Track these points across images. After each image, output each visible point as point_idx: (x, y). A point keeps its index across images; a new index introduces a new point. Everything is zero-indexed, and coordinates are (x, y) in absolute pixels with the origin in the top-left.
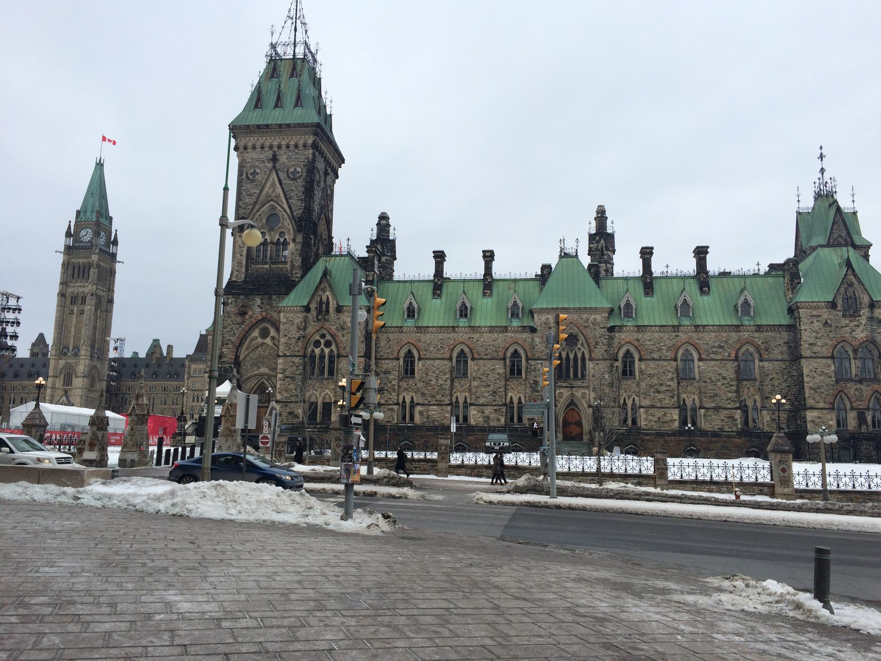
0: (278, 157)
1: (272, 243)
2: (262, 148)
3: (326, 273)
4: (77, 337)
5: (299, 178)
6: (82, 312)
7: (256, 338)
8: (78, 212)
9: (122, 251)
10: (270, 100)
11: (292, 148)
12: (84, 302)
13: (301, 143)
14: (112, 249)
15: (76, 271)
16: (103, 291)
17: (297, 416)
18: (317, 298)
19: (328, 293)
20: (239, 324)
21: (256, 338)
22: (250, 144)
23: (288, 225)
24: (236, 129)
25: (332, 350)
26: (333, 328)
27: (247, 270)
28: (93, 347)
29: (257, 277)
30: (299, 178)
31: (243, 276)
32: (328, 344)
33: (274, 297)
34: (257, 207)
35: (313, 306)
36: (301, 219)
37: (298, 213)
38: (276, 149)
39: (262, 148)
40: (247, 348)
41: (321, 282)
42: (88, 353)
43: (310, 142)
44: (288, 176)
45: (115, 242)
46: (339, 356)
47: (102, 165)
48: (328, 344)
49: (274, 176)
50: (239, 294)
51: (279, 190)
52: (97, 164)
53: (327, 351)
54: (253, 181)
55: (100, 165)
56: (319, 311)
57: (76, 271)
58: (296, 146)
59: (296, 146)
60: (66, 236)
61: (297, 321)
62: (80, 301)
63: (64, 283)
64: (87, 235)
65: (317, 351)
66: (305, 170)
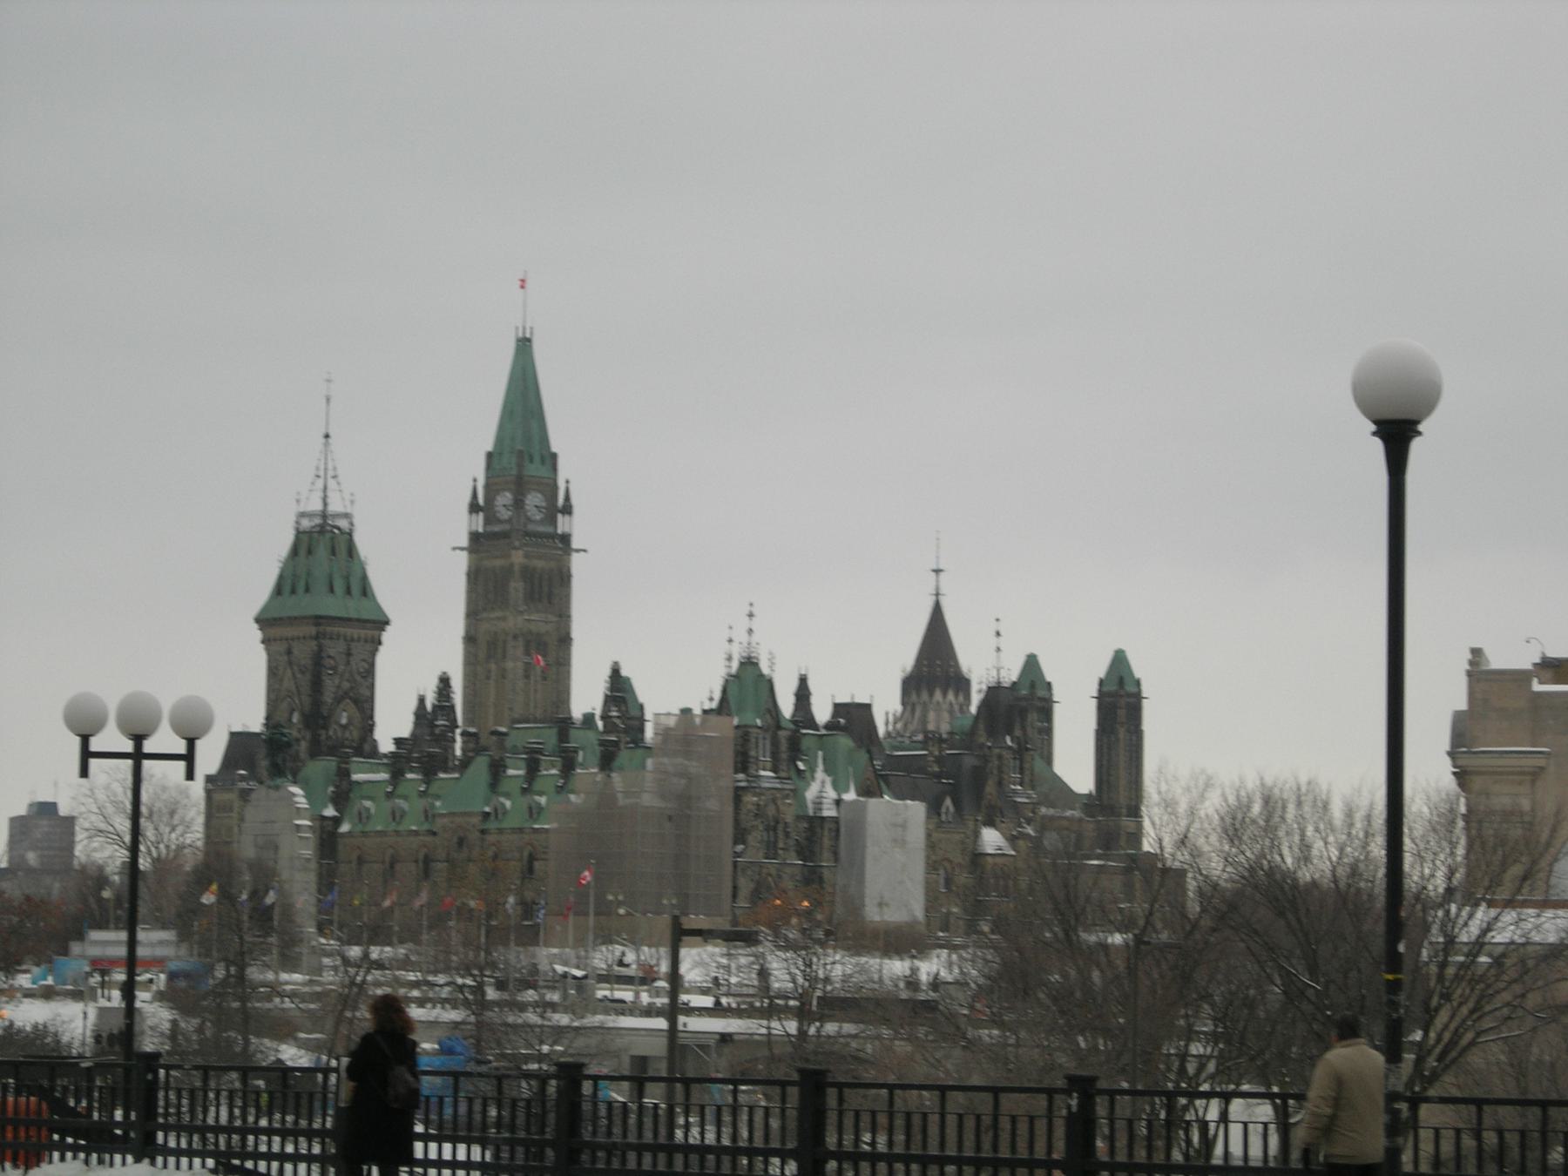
8: (490, 456)
10: (287, 589)
24: (263, 621)
45: (567, 510)
47: (529, 340)
52: (519, 340)
55: (524, 346)
63: (472, 614)
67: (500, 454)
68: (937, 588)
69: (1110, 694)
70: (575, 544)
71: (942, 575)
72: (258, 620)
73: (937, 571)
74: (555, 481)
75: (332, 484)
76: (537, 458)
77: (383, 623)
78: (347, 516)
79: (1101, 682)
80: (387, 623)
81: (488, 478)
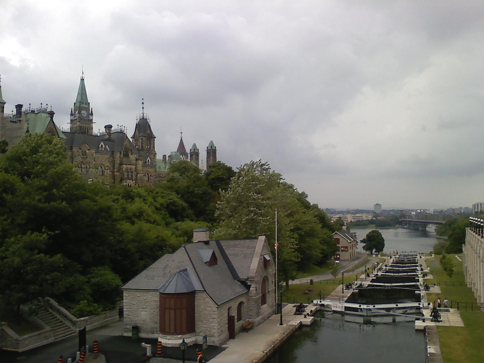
45: (92, 114)
47: (83, 79)
52: (81, 79)
55: (82, 80)
67: (77, 103)
68: (181, 136)
69: (209, 150)
71: (182, 134)
73: (181, 133)
74: (89, 108)
76: (85, 103)
79: (207, 148)
81: (74, 108)
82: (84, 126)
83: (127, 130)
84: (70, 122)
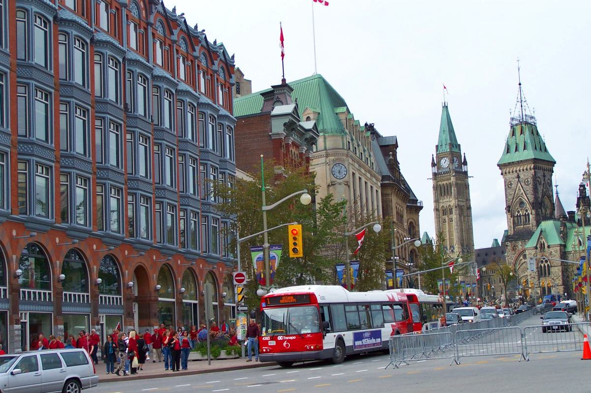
0: (520, 176)
1: (523, 215)
2: (513, 172)
3: (541, 231)
4: (451, 240)
5: (530, 184)
6: (451, 220)
7: (522, 259)
8: (437, 146)
9: (470, 169)
10: (513, 148)
11: (525, 170)
12: (451, 213)
13: (528, 167)
14: (464, 168)
15: (443, 190)
16: (463, 202)
17: (538, 293)
18: (539, 243)
19: (543, 240)
20: (514, 254)
21: (522, 259)
22: (507, 171)
23: (528, 206)
25: (548, 264)
26: (547, 255)
27: (514, 229)
28: (462, 245)
29: (518, 232)
30: (530, 184)
31: (513, 232)
32: (546, 261)
33: (526, 241)
34: (514, 200)
35: (538, 246)
36: (533, 203)
37: (531, 200)
38: (518, 172)
39: (513, 172)
40: (519, 264)
41: (540, 236)
42: (460, 250)
43: (532, 166)
44: (525, 184)
45: (465, 163)
46: (551, 267)
47: (447, 107)
48: (546, 261)
49: (519, 184)
50: (512, 241)
51: (522, 191)
52: (443, 107)
53: (546, 265)
54: (511, 188)
55: (445, 107)
56: (541, 247)
57: (443, 190)
58: (527, 169)
59: (527, 169)
60: (432, 167)
61: (533, 253)
62: (449, 212)
63: (437, 201)
64: (445, 163)
65: (542, 265)
66: (532, 180)
70: (469, 175)
71: (558, 187)
72: (498, 165)
74: (460, 153)
75: (524, 104)
76: (454, 146)
77: (553, 163)
78: (532, 118)
80: (555, 163)
81: (437, 154)
82: (446, 184)
83: (556, 186)
84: (431, 177)
